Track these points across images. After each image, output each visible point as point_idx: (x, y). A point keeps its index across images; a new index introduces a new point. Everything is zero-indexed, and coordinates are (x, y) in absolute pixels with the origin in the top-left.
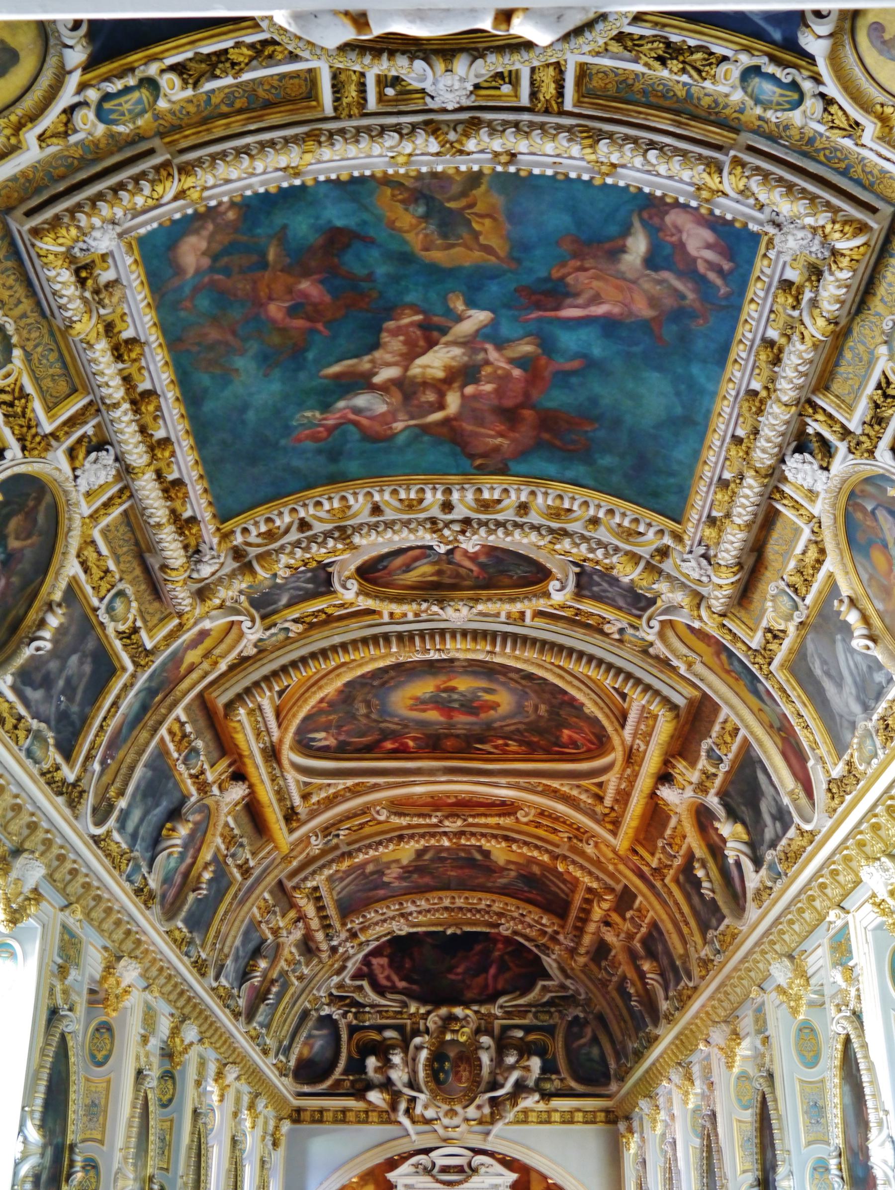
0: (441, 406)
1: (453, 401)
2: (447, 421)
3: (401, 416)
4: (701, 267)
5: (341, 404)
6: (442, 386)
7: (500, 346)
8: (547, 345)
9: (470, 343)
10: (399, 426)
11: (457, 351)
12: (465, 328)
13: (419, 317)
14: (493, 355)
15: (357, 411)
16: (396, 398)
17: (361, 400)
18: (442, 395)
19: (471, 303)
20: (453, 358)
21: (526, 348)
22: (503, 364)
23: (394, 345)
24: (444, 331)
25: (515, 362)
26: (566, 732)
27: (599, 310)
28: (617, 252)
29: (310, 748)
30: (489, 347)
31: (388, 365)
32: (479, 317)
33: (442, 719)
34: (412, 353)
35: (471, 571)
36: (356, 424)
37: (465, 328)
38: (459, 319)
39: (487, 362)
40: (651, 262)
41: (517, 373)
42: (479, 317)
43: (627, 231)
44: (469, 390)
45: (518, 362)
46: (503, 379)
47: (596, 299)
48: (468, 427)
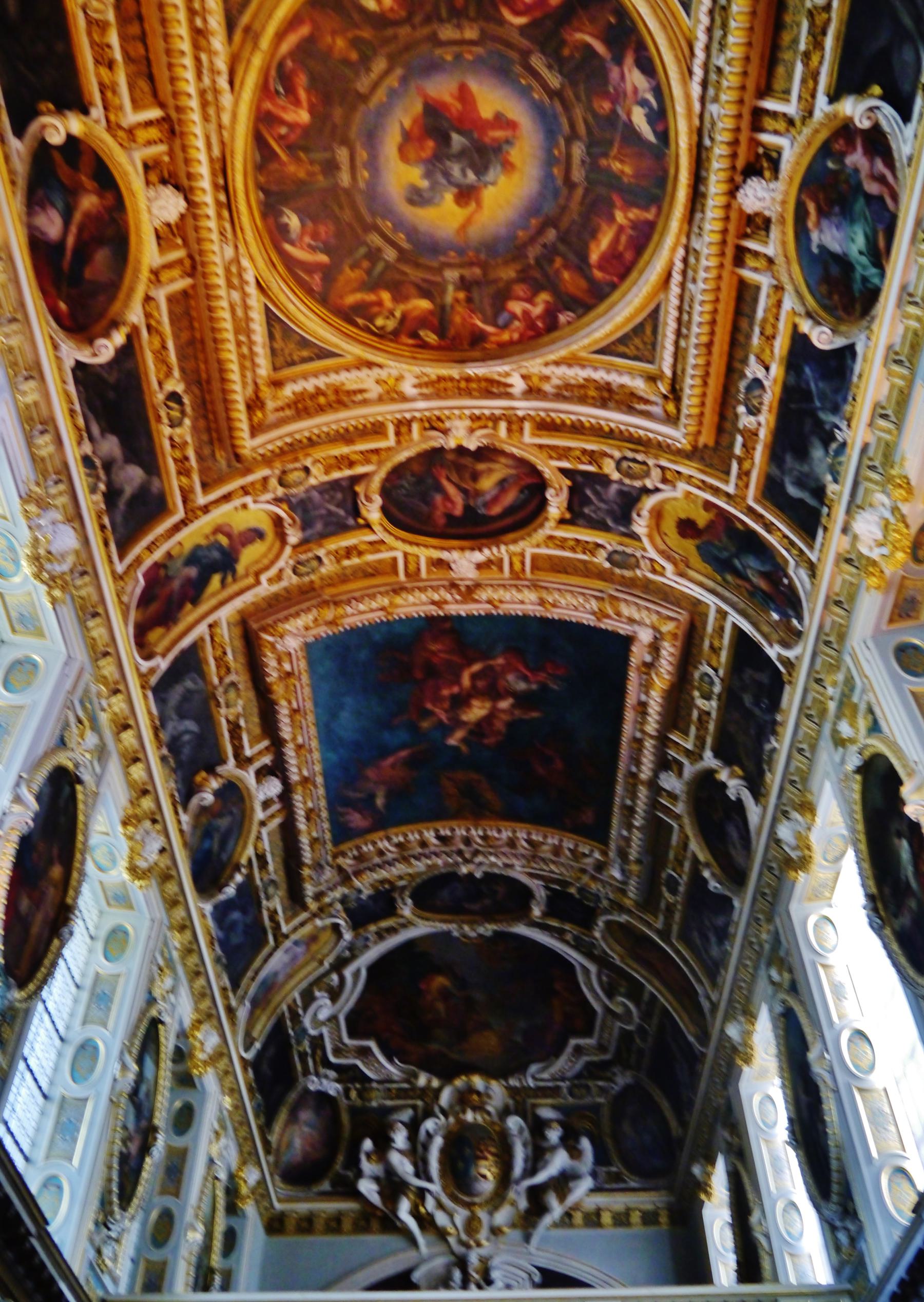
0: (474, 677)
1: (466, 681)
2: (470, 663)
3: (498, 669)
4: (350, 810)
5: (534, 687)
6: (474, 693)
7: (441, 722)
8: (413, 728)
9: (458, 723)
10: (500, 661)
11: (465, 718)
12: (460, 734)
13: (486, 741)
14: (443, 717)
15: (525, 678)
16: (502, 683)
17: (522, 686)
18: (473, 686)
19: (455, 749)
20: (465, 712)
21: (425, 725)
22: (437, 710)
23: (499, 725)
24: (471, 732)
25: (430, 713)
26: (304, 116)
27: (390, 760)
28: (389, 796)
29: (658, 91)
30: (445, 720)
31: (503, 711)
32: (452, 742)
33: (474, 86)
34: (488, 719)
35: (449, 479)
36: (527, 667)
37: (460, 734)
38: (464, 740)
39: (446, 711)
40: (372, 797)
41: (429, 706)
42: (452, 742)
43: (387, 806)
44: (456, 690)
45: (429, 714)
46: (437, 700)
47: (393, 766)
48: (456, 659)
